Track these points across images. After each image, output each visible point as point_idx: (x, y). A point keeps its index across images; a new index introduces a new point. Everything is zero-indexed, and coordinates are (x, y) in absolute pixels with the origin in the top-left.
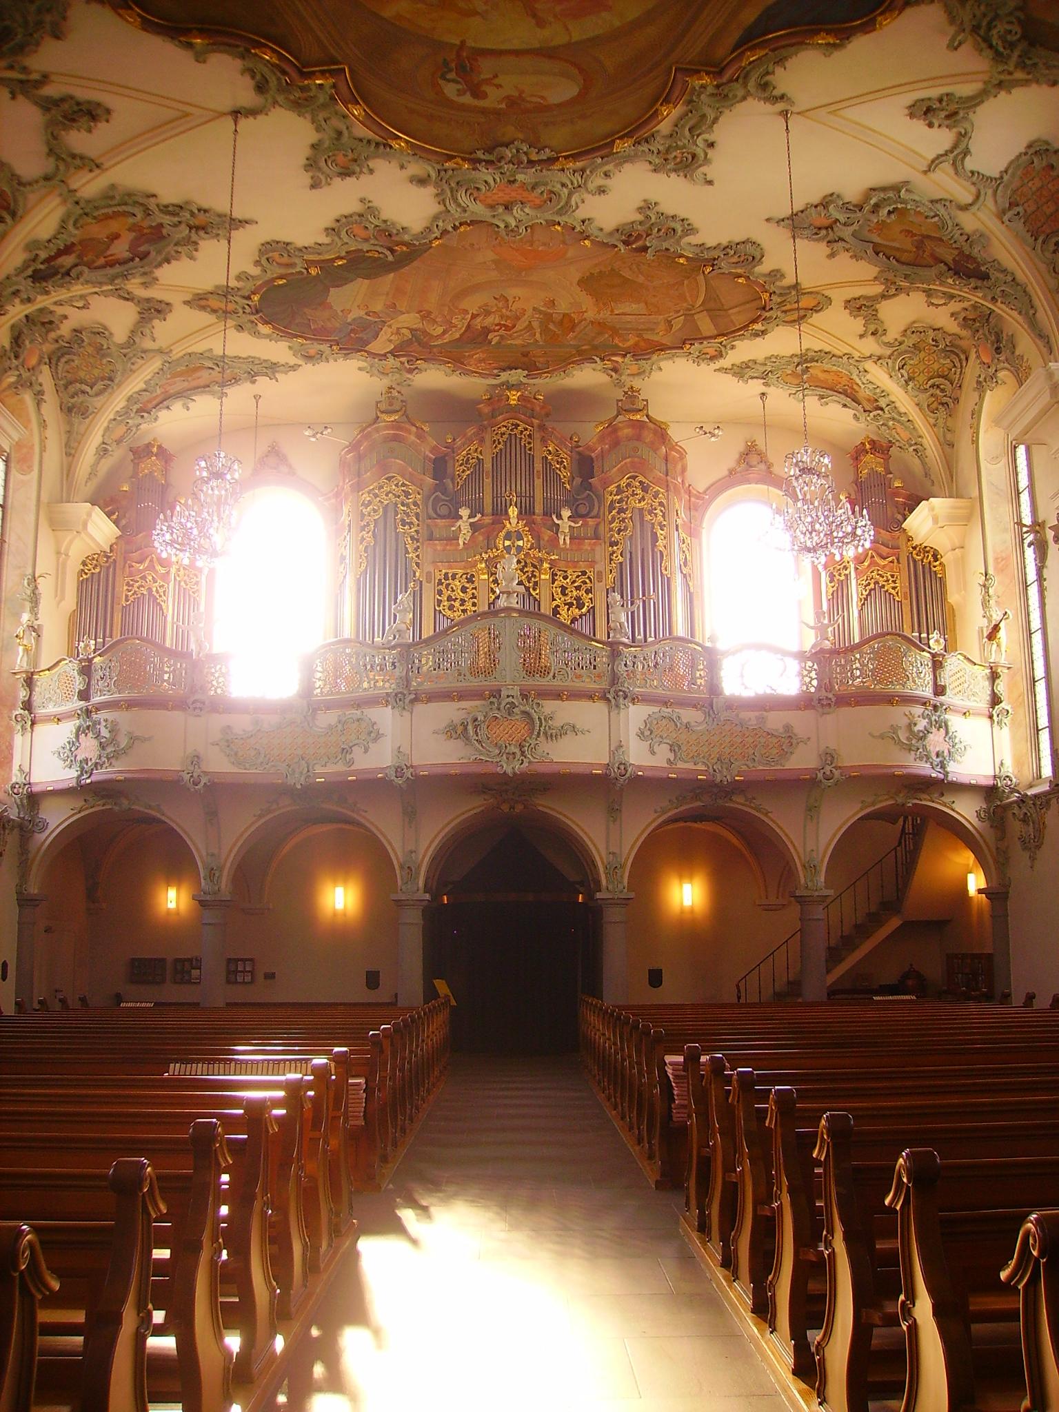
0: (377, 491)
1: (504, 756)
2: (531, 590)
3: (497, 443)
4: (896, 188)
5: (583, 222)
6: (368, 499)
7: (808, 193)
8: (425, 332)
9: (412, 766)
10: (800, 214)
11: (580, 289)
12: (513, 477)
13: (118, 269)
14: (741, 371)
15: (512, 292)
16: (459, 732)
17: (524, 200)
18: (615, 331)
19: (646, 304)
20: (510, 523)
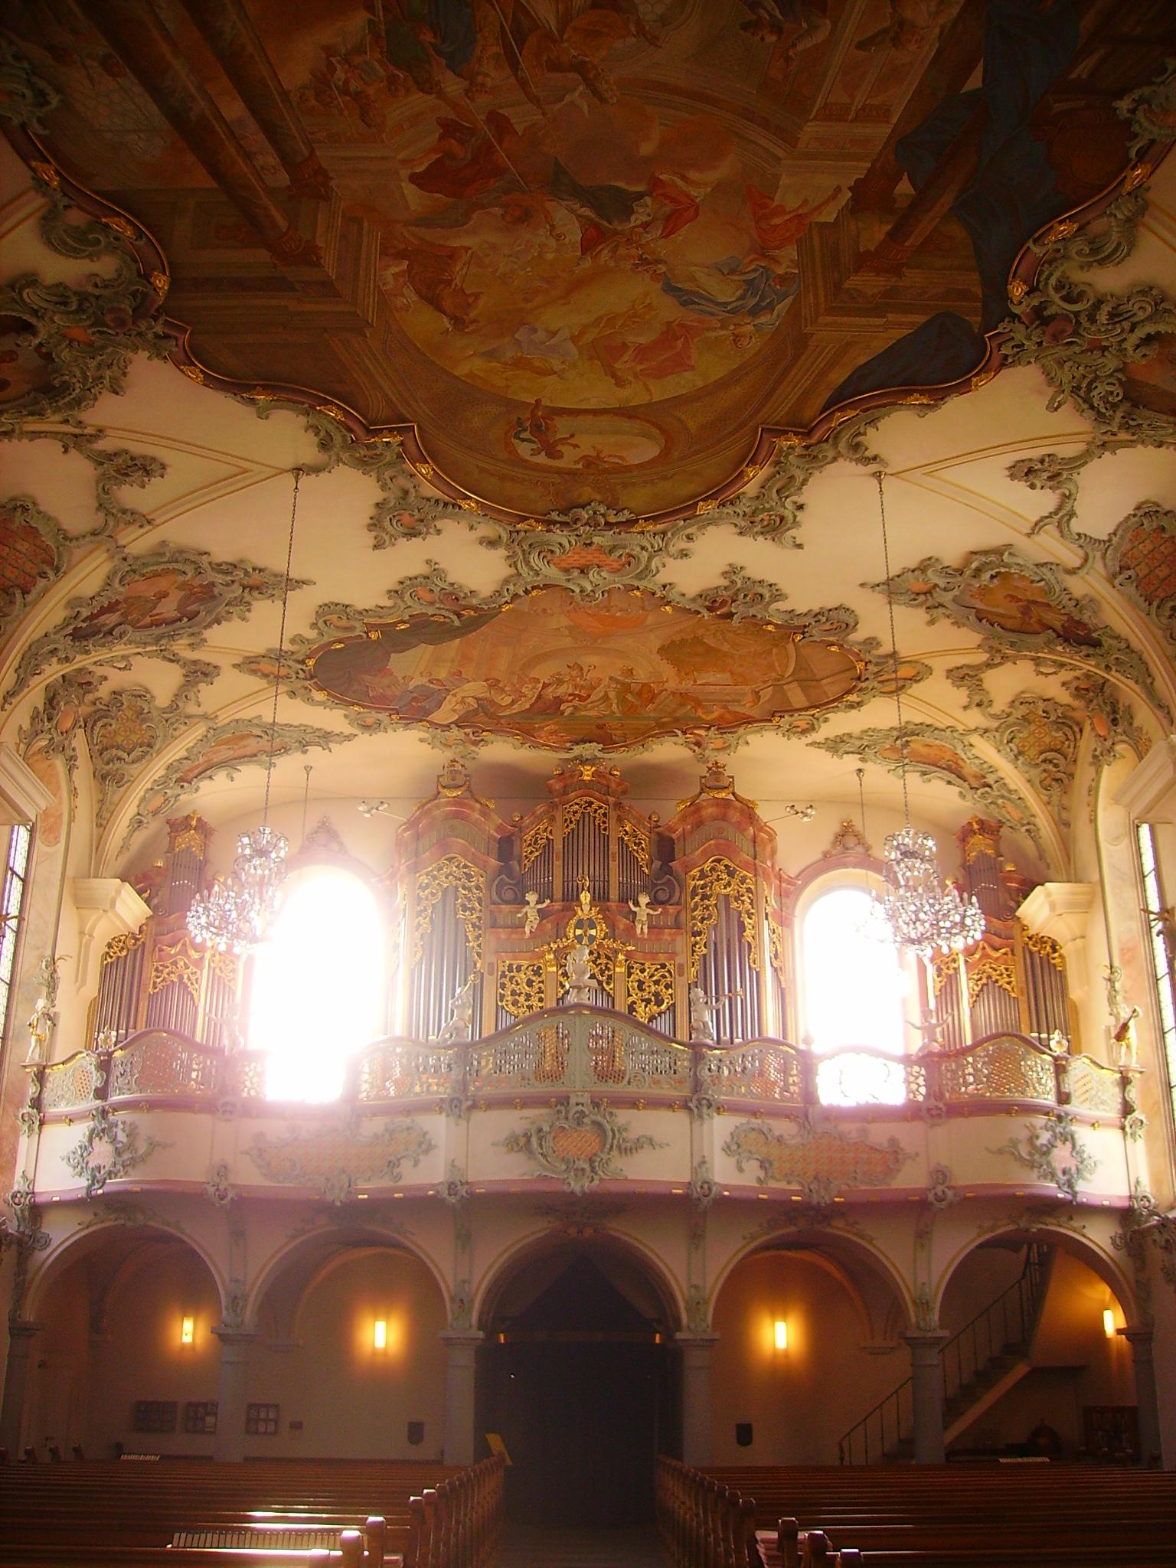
1: (572, 1174)
4: (998, 552)
5: (664, 586)
7: (905, 557)
8: (492, 702)
9: (467, 1183)
12: (586, 859)
13: (163, 629)
14: (836, 745)
15: (588, 660)
16: (521, 1144)
17: (601, 564)
18: (698, 703)
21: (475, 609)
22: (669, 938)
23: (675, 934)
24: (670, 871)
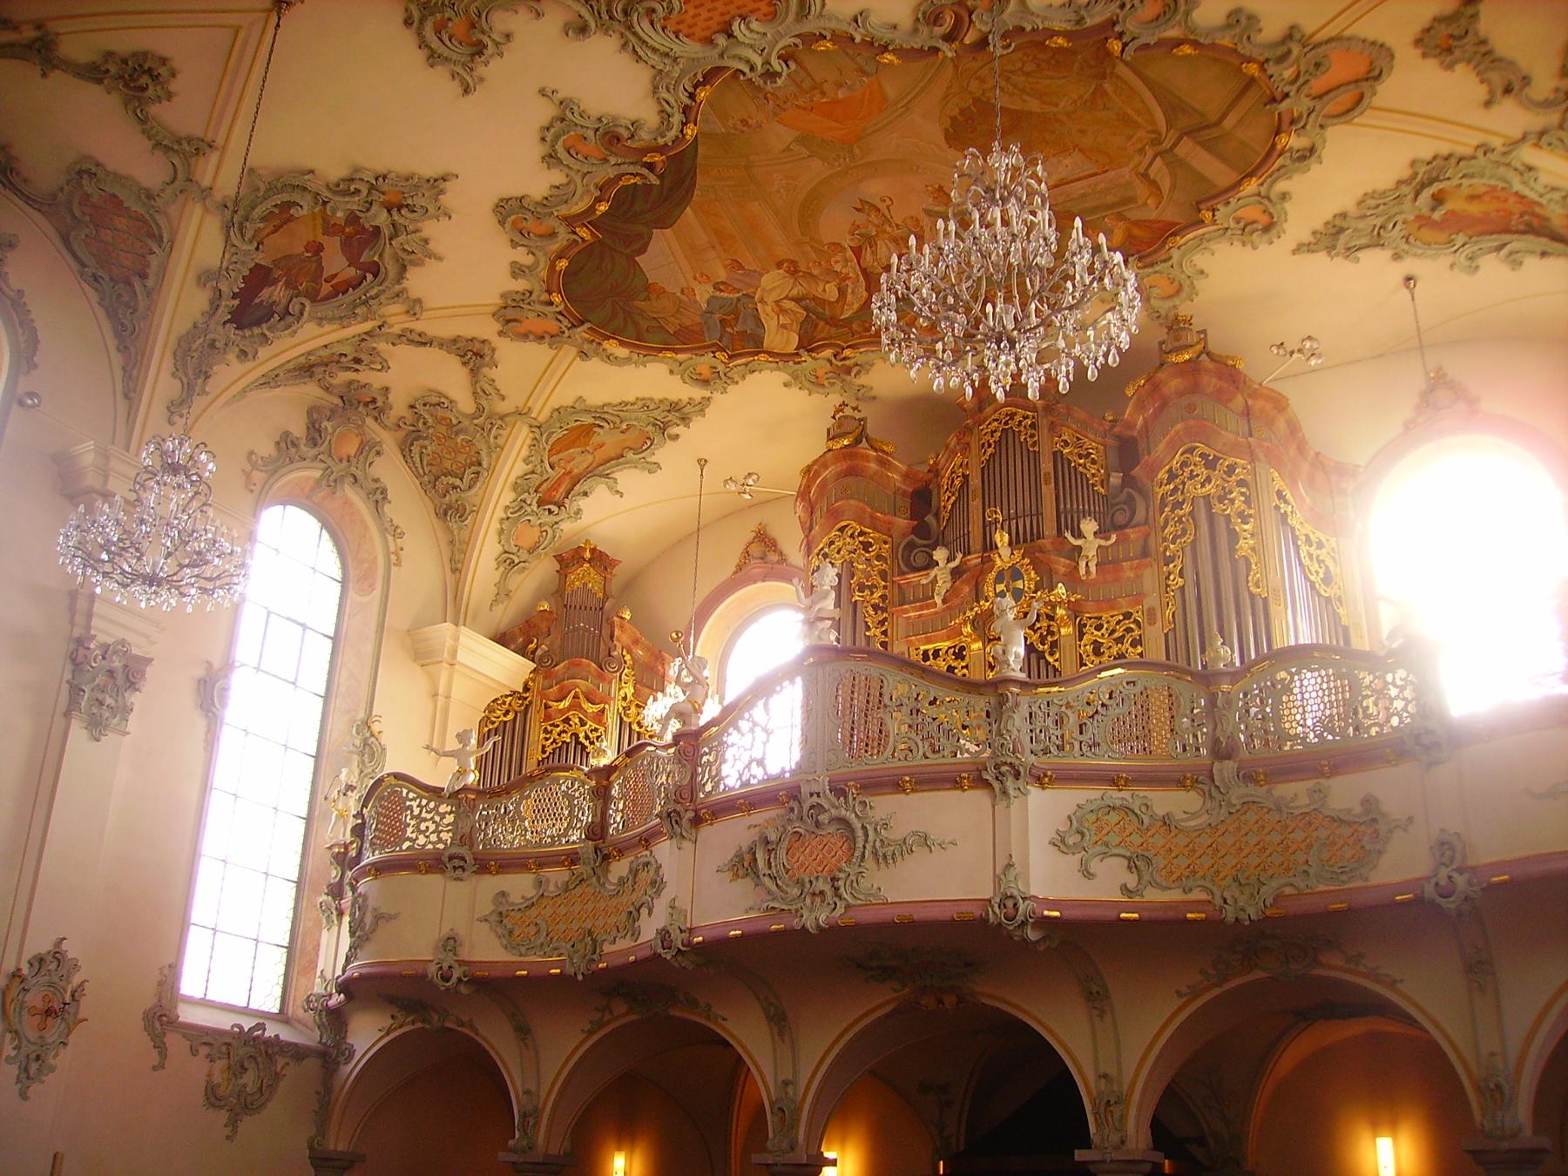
0: (826, 550)
2: (1047, 655)
3: (986, 445)
17: (743, 11)
19: (1080, 150)
20: (1000, 556)
22: (1132, 575)
23: (1139, 567)
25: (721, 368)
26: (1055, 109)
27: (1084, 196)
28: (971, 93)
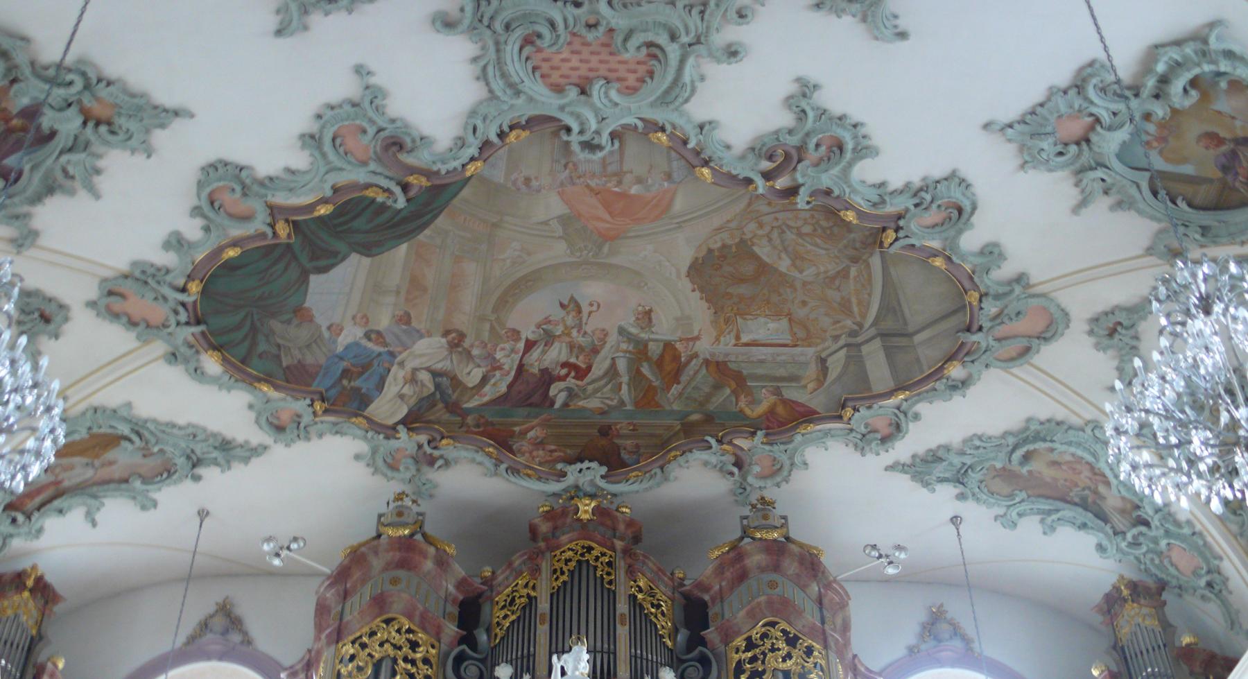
3: (558, 573)
4: (1199, 37)
5: (701, 127)
6: (352, 651)
8: (456, 382)
10: (1039, 110)
11: (689, 286)
15: (592, 291)
19: (790, 320)
21: (428, 174)
24: (703, 642)
25: (307, 419)
26: (797, 275)
27: (762, 362)
28: (744, 233)
